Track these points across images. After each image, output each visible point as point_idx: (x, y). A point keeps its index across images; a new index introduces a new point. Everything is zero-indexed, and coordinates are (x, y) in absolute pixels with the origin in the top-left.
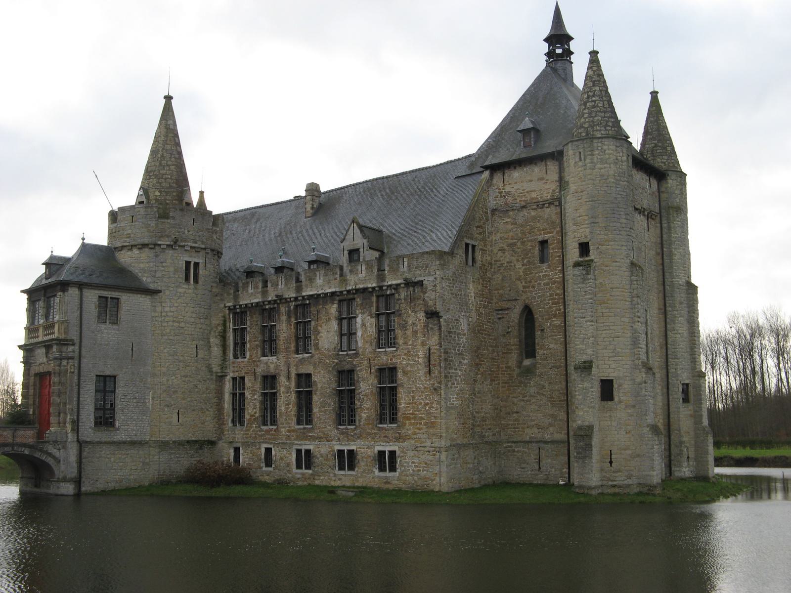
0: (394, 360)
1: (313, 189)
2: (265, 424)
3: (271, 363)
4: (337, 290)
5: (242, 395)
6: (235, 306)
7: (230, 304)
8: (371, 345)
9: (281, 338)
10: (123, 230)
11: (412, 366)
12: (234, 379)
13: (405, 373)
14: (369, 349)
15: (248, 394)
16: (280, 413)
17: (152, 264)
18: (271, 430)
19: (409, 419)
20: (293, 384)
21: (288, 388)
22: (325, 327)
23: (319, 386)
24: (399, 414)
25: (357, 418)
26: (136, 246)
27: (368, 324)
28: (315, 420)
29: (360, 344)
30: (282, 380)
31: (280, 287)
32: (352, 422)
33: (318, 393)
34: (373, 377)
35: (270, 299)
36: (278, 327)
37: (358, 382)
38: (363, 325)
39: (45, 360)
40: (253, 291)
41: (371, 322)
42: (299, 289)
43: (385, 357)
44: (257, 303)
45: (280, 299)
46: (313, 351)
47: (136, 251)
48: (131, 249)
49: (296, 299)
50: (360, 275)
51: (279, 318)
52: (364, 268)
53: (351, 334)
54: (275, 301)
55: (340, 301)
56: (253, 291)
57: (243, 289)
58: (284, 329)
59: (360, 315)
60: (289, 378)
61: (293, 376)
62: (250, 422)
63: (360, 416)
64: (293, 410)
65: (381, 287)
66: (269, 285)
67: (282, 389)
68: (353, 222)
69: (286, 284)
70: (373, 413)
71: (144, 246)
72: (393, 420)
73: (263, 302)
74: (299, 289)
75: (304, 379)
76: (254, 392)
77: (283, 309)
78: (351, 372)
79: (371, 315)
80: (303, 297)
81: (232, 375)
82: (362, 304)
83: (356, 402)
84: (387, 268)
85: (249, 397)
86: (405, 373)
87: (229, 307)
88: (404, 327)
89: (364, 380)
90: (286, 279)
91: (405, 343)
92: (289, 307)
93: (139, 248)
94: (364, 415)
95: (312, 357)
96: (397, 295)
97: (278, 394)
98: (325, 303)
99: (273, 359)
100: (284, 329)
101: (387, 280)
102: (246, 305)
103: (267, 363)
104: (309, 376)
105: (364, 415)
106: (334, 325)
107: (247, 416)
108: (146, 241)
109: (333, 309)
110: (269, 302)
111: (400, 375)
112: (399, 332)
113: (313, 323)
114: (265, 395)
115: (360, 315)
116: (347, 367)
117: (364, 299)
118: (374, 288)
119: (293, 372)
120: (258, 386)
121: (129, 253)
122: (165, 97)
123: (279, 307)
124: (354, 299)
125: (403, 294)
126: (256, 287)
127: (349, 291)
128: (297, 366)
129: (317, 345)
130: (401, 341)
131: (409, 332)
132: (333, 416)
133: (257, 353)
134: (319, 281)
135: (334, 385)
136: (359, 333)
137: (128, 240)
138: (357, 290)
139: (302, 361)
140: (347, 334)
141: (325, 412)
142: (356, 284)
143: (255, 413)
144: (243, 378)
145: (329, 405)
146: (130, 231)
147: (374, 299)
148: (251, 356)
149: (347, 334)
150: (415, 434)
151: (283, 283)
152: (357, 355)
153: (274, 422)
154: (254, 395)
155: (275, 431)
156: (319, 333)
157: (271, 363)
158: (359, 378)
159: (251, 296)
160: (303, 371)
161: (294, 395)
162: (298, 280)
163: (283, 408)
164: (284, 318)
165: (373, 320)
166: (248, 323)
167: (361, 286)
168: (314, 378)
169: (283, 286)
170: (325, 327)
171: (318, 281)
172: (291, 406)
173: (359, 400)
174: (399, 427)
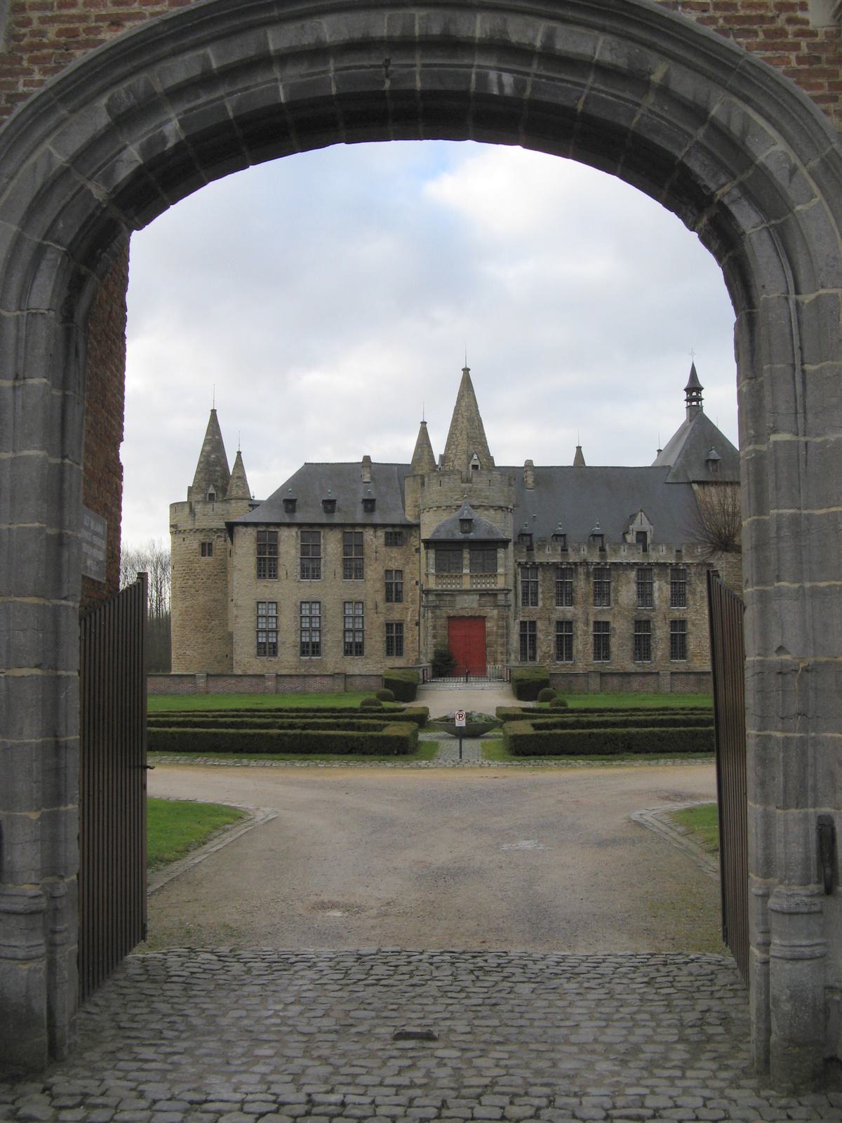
0: (685, 616)
1: (529, 464)
2: (559, 658)
3: (568, 611)
4: (640, 561)
5: (534, 638)
6: (526, 563)
7: (523, 560)
8: (667, 603)
9: (579, 593)
10: (481, 490)
11: (699, 620)
12: (523, 624)
13: (694, 625)
14: (665, 606)
15: (540, 635)
16: (577, 652)
17: (503, 524)
18: (567, 664)
19: (696, 656)
20: (591, 628)
21: (586, 633)
22: (624, 587)
23: (618, 631)
24: (689, 653)
25: (653, 655)
26: (492, 507)
27: (664, 589)
28: (612, 656)
29: (657, 602)
30: (580, 628)
31: (582, 552)
32: (648, 658)
33: (616, 636)
34: (667, 626)
35: (571, 561)
36: (575, 584)
37: (655, 629)
38: (660, 589)
39: (475, 605)
40: (550, 552)
41: (667, 589)
42: (603, 557)
43: (677, 612)
44: (554, 563)
45: (585, 563)
46: (612, 604)
47: (492, 511)
48: (487, 510)
49: (598, 564)
50: (661, 553)
51: (577, 577)
52: (664, 548)
53: (651, 595)
54: (575, 564)
55: (638, 570)
56: (550, 552)
57: (539, 550)
58: (582, 585)
59: (657, 582)
60: (587, 624)
61: (591, 623)
62: (543, 658)
63: (656, 654)
64: (590, 648)
65: (677, 564)
66: (570, 550)
67: (579, 633)
68: (641, 511)
69: (589, 552)
70: (667, 652)
71: (500, 508)
72: (683, 657)
73: (561, 563)
74: (603, 557)
75: (602, 628)
76: (548, 634)
77: (581, 570)
78: (648, 622)
79: (666, 582)
80: (606, 564)
81: (521, 619)
82: (659, 574)
83: (652, 644)
84: (684, 551)
85: (542, 637)
86: (694, 625)
87: (520, 563)
88: (694, 593)
89: (659, 628)
90: (589, 547)
91: (694, 604)
92: (588, 569)
93: (495, 510)
94: (659, 653)
95: (611, 609)
96: (688, 571)
97: (574, 637)
98: (627, 569)
99: (571, 608)
100: (582, 585)
101: (684, 559)
102: (541, 563)
103: (563, 612)
104: (607, 623)
105: (659, 653)
106: (634, 587)
107: (539, 654)
108: (502, 504)
109: (633, 574)
110: (568, 563)
111: (689, 626)
112: (689, 596)
113: (613, 584)
114: (558, 636)
115: (657, 582)
116: (645, 618)
117: (660, 570)
118: (671, 564)
119: (592, 619)
120: (552, 629)
121: (486, 512)
122: (463, 370)
123: (576, 569)
124: (651, 569)
125: (693, 570)
126: (554, 549)
127: (649, 564)
128: (595, 615)
129: (617, 602)
130: (691, 603)
131: (698, 597)
132: (631, 654)
133: (551, 602)
134: (623, 553)
135: (632, 631)
136: (656, 595)
137: (486, 501)
138: (657, 564)
139: (601, 612)
140: (644, 593)
141: (623, 650)
142: (658, 559)
143: (550, 650)
144: (533, 624)
145: (627, 646)
146: (488, 494)
147: (669, 571)
148: (544, 605)
149: (644, 593)
150: (701, 666)
151: (586, 550)
152: (654, 610)
153: (570, 657)
154: (547, 636)
155: (572, 665)
156: (620, 591)
157: (568, 611)
158: (655, 626)
159: (548, 555)
160: (602, 619)
161: (591, 639)
162: (602, 549)
163: (580, 647)
164: (582, 577)
165: (669, 586)
166: (540, 577)
167: (662, 561)
168: (612, 625)
169: (585, 553)
170: (624, 587)
171: (622, 553)
172: (589, 646)
173: (655, 642)
174: (688, 662)
